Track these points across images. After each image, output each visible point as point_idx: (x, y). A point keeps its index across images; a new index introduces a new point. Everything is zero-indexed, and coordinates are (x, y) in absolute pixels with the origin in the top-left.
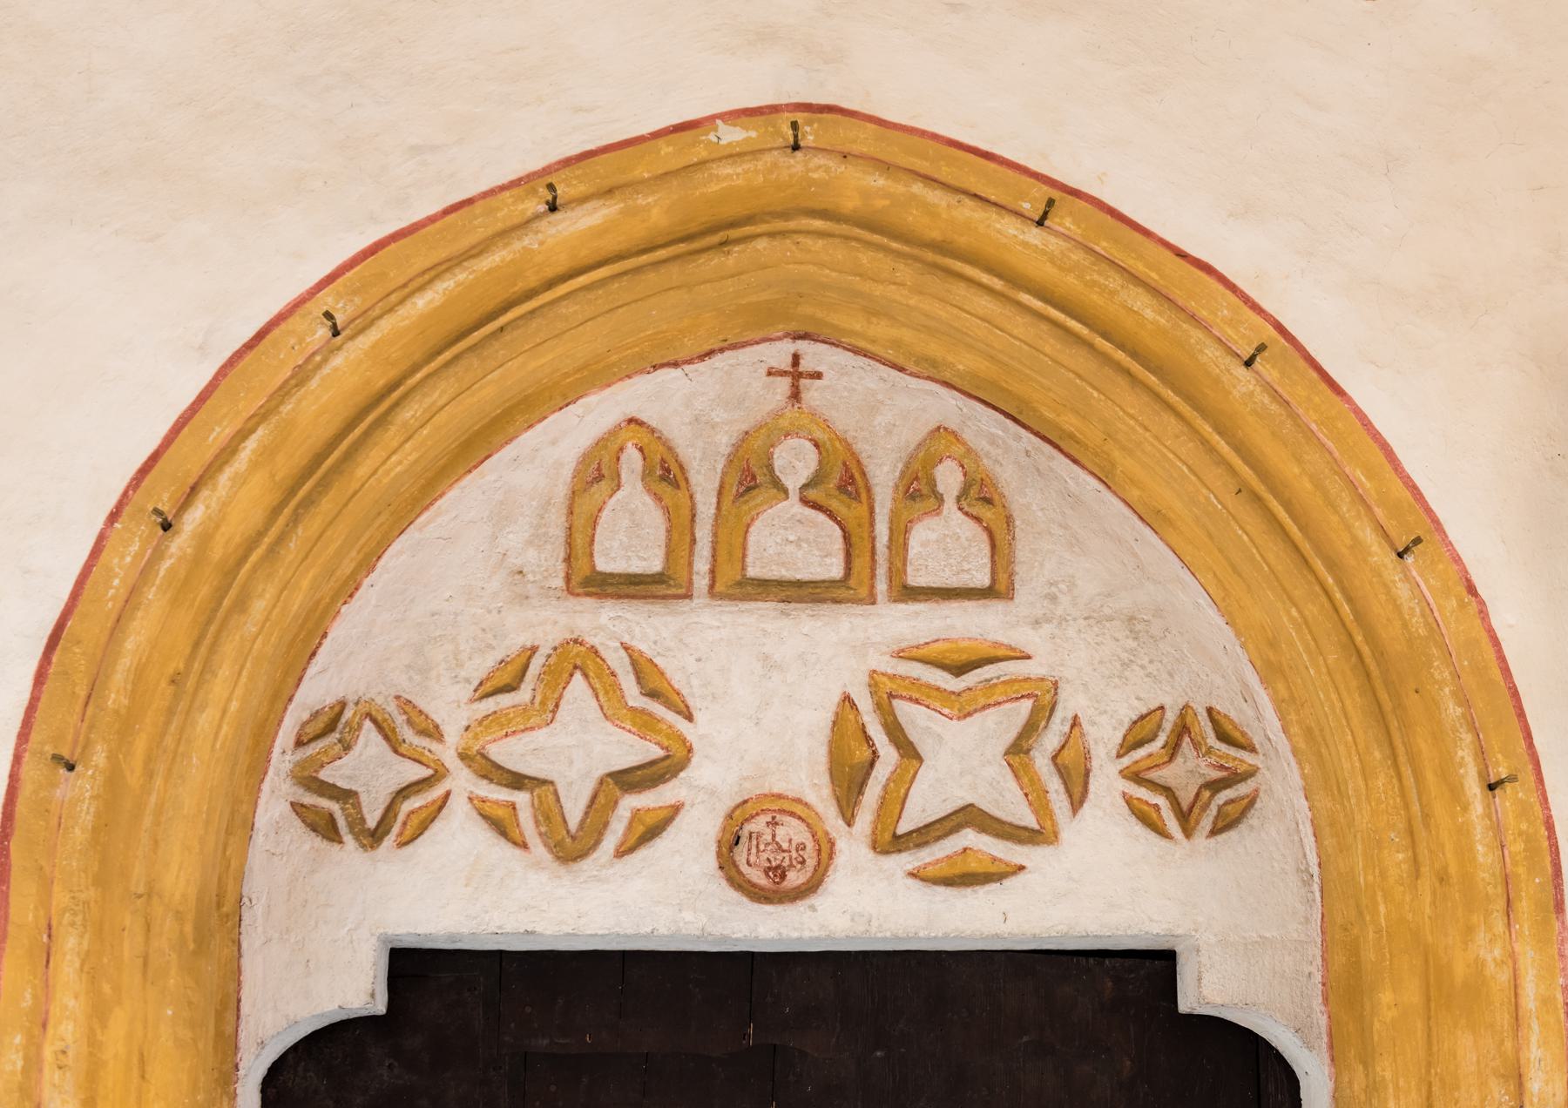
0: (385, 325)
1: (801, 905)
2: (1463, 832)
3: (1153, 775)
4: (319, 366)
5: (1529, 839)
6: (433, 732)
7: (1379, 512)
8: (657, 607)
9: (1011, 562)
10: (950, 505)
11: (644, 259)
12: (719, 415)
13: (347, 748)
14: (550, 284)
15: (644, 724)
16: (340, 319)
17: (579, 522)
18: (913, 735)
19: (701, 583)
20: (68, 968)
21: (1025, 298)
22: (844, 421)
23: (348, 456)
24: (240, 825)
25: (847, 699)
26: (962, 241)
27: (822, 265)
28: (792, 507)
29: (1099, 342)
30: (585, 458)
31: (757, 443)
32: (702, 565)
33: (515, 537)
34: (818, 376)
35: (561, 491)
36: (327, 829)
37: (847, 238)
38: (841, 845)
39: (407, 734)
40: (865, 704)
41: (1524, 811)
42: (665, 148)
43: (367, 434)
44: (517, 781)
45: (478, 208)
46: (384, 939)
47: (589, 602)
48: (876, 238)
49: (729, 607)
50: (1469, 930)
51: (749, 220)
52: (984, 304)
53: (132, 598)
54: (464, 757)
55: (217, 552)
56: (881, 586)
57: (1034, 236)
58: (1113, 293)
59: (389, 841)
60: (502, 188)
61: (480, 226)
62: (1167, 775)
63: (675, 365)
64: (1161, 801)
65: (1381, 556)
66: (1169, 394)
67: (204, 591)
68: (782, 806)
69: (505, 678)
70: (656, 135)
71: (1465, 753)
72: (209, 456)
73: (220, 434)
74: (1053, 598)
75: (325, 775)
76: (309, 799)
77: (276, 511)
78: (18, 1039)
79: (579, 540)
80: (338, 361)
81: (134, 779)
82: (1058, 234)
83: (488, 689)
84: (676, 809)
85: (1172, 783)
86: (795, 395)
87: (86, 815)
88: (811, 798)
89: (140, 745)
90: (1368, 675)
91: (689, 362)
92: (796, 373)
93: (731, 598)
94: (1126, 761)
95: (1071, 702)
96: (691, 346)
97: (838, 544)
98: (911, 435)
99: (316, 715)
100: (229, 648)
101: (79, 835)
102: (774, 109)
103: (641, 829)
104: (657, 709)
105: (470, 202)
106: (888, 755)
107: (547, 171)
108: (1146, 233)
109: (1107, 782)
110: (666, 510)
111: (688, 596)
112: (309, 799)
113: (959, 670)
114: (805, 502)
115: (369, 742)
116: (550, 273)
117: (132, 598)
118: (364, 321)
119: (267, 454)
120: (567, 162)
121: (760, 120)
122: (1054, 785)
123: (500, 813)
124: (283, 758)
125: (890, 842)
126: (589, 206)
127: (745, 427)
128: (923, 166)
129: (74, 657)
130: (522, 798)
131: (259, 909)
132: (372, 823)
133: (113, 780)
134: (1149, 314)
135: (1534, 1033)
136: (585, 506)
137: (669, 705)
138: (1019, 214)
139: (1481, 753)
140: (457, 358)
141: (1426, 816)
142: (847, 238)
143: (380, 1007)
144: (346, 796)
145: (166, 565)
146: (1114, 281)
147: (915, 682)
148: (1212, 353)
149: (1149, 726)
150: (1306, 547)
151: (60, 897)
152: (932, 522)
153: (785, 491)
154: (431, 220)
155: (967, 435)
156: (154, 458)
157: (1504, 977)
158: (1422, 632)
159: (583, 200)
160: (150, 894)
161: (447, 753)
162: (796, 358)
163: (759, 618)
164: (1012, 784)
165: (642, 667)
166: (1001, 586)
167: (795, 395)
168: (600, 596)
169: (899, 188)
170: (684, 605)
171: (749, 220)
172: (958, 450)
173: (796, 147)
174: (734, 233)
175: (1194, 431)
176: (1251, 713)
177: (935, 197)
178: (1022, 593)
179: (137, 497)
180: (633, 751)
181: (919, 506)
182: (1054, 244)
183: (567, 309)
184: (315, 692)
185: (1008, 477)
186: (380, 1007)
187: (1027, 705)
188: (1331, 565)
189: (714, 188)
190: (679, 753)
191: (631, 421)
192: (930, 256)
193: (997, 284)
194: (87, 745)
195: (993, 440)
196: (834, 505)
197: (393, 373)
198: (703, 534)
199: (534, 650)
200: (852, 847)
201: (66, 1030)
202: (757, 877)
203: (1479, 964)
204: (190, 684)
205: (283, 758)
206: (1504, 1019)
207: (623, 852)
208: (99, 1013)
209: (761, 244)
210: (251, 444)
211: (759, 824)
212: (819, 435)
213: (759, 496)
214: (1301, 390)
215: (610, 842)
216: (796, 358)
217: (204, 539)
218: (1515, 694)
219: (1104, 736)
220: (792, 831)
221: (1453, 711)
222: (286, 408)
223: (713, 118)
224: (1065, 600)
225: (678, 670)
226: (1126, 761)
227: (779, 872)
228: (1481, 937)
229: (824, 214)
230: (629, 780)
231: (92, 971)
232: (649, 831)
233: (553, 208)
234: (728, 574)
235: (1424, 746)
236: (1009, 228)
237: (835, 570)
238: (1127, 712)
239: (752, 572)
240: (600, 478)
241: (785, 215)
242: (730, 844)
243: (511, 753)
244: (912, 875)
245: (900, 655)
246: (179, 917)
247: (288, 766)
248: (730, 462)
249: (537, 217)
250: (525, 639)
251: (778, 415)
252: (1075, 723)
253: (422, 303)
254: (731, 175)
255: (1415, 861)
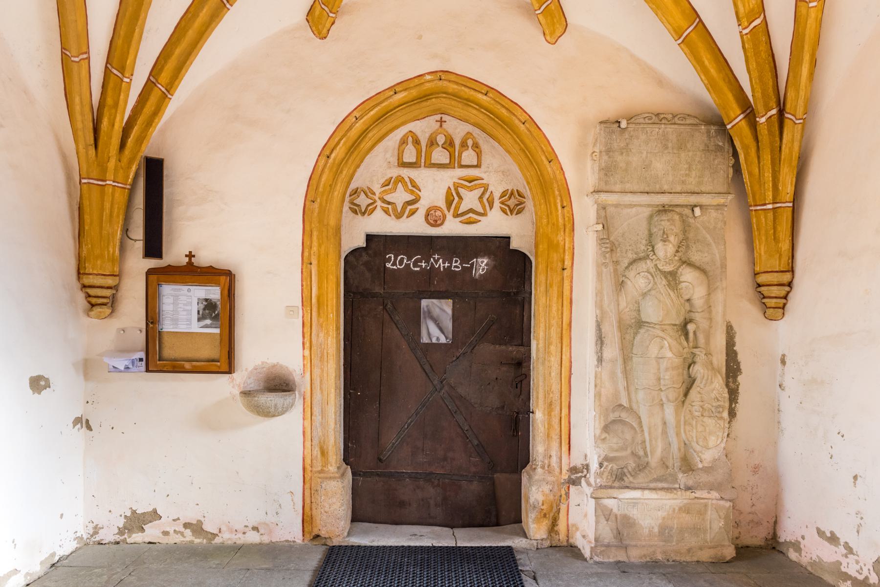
0: (365, 118)
1: (440, 227)
2: (557, 216)
3: (506, 203)
4: (354, 126)
5: (569, 217)
6: (374, 194)
7: (546, 154)
8: (414, 169)
9: (481, 160)
10: (470, 148)
11: (412, 103)
12: (426, 130)
13: (359, 197)
14: (395, 108)
15: (412, 192)
16: (357, 117)
17: (400, 151)
18: (462, 195)
19: (423, 164)
20: (315, 238)
21: (483, 110)
22: (450, 131)
23: (359, 143)
24: (341, 211)
25: (449, 188)
26: (471, 98)
27: (444, 104)
28: (440, 149)
29: (496, 119)
30: (401, 139)
31: (434, 136)
32: (423, 161)
33: (388, 155)
34: (445, 122)
35: (397, 146)
36: (355, 212)
37: (449, 98)
38: (447, 216)
39: (369, 194)
40: (452, 189)
41: (568, 212)
42: (416, 80)
43: (362, 139)
44: (389, 203)
45: (382, 94)
46: (366, 233)
47: (402, 168)
48: (455, 98)
49: (428, 169)
50: (558, 234)
51: (432, 94)
52: (475, 112)
53: (323, 170)
54: (379, 198)
55: (336, 162)
56: (456, 165)
57: (485, 98)
58: (499, 109)
59: (366, 214)
60: (387, 89)
61: (382, 97)
62: (508, 203)
63: (418, 120)
64: (507, 208)
65: (546, 162)
66: (509, 130)
67: (335, 169)
68: (437, 208)
69: (387, 183)
70: (415, 78)
71: (558, 201)
72: (335, 143)
73: (337, 139)
74: (488, 167)
75: (355, 202)
76: (352, 206)
77: (347, 154)
78: (307, 250)
79: (400, 155)
80: (357, 125)
81: (324, 204)
82: (489, 97)
83: (384, 185)
84: (417, 209)
85: (509, 204)
86: (441, 126)
87: (317, 211)
88: (442, 207)
89: (325, 198)
90: (542, 186)
91: (421, 119)
92: (441, 121)
93: (428, 167)
94: (501, 200)
95: (491, 188)
96: (421, 117)
97: (449, 156)
98: (462, 134)
99: (353, 190)
100: (340, 180)
101: (316, 214)
102: (436, 72)
103: (411, 212)
104: (414, 189)
105: (380, 93)
106: (456, 199)
107: (395, 86)
108: (506, 97)
109: (497, 204)
110: (417, 149)
111: (420, 167)
112: (352, 206)
113: (470, 182)
114: (443, 147)
115: (363, 196)
116: (395, 106)
117: (323, 170)
118: (362, 117)
119: (345, 143)
120: (398, 84)
121: (433, 74)
122: (487, 205)
123: (386, 209)
124: (347, 199)
125: (456, 215)
126: (402, 92)
127: (431, 132)
128: (464, 83)
129: (314, 182)
130: (390, 207)
131: (344, 227)
132: (363, 211)
133: (321, 205)
134: (505, 113)
135: (567, 253)
136: (401, 149)
137: (416, 189)
138: (482, 93)
139: (562, 201)
140: (378, 124)
141: (551, 213)
142: (449, 98)
143: (365, 246)
144: (358, 206)
145: (328, 165)
146: (499, 107)
147: (462, 184)
148: (517, 122)
149: (506, 193)
150: (532, 160)
151: (313, 225)
152: (466, 152)
153: (439, 145)
154: (374, 96)
155: (474, 134)
156: (326, 144)
157: (562, 243)
158: (552, 177)
159: (401, 91)
160: (328, 224)
161: (377, 199)
162: (441, 118)
163: (433, 172)
164: (480, 204)
165: (412, 181)
166: (479, 165)
167: (441, 126)
168: (404, 167)
169: (460, 88)
170: (419, 169)
171: (432, 94)
172: (472, 137)
173: (440, 79)
174: (428, 97)
175: (513, 137)
176: (524, 190)
177: (466, 90)
178: (483, 166)
179: (323, 152)
180: (410, 197)
181: (464, 148)
182: (488, 99)
183: (398, 114)
184: (353, 186)
185: (481, 143)
186: (365, 246)
187: (483, 188)
188: (537, 164)
189: (425, 88)
190: (418, 198)
191: (410, 131)
192: (465, 102)
193: (477, 107)
194: (316, 198)
195: (478, 135)
196: (448, 148)
197: (366, 127)
198: (423, 155)
199: (392, 178)
200: (449, 216)
201: (315, 249)
202: (432, 222)
203: (558, 240)
204: (333, 187)
205: (347, 199)
206: (561, 251)
207: (407, 217)
208: (320, 246)
209: (434, 100)
210: (342, 141)
211: (432, 212)
212: (445, 134)
213: (434, 147)
214: (533, 129)
215: (405, 215)
216: (441, 118)
217: (335, 159)
218: (568, 190)
219: (497, 195)
220: (438, 213)
221: (557, 193)
222: (348, 134)
223: (425, 74)
224: (491, 168)
225: (418, 181)
226: (501, 200)
227: (436, 221)
228: (559, 236)
229: (445, 93)
230: (410, 203)
231: (318, 239)
232: (413, 213)
233: (395, 93)
234: (428, 162)
235: (552, 199)
236: (480, 96)
237: (448, 161)
238: (501, 190)
239: (432, 162)
240: (404, 143)
241: (438, 93)
242: (427, 215)
243: (388, 198)
244: (460, 222)
245: (460, 179)
246: (333, 229)
247: (348, 200)
248: (428, 139)
249: (393, 95)
250: (389, 176)
251: (437, 130)
252: (492, 192)
253: (372, 113)
254: (428, 85)
255: (548, 221)
